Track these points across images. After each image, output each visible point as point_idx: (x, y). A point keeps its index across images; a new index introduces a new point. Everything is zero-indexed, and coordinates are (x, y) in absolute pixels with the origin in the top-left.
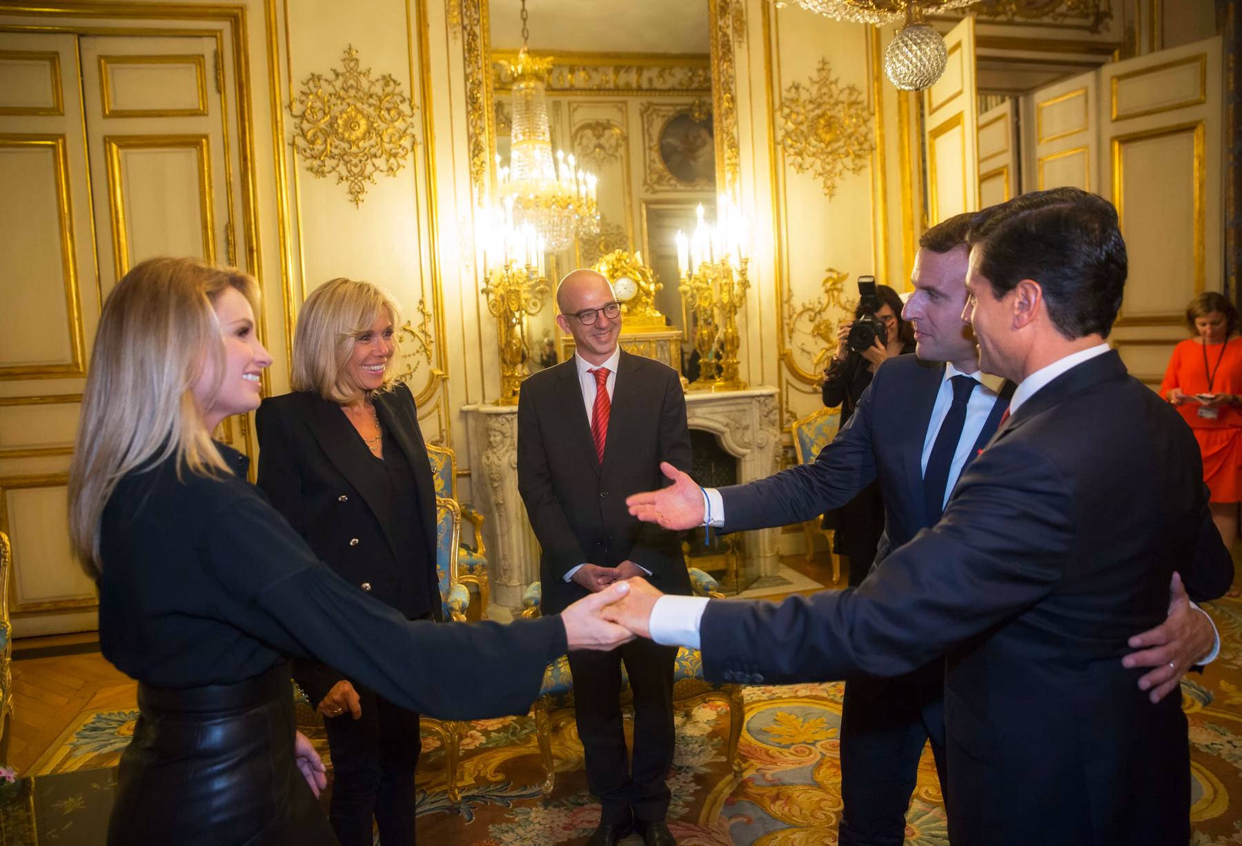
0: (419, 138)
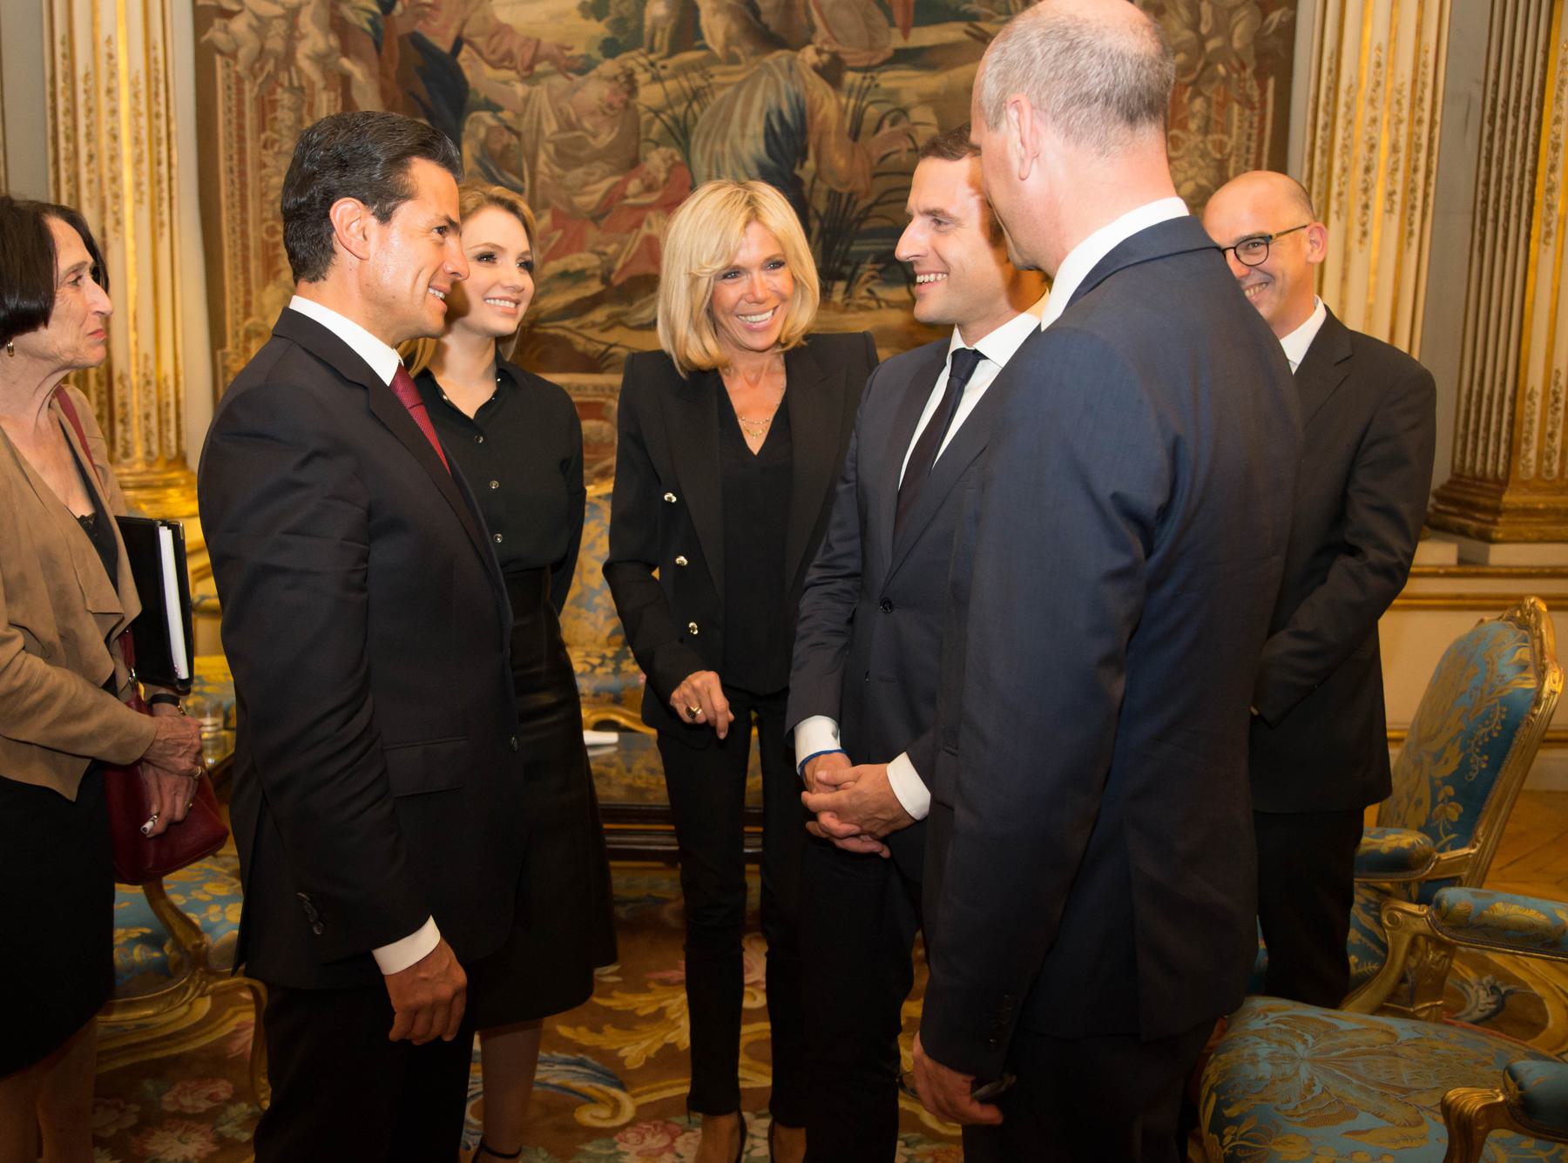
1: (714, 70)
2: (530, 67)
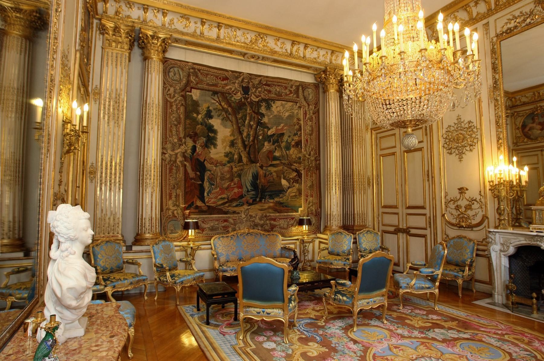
0: (480, 139)
1: (244, 166)
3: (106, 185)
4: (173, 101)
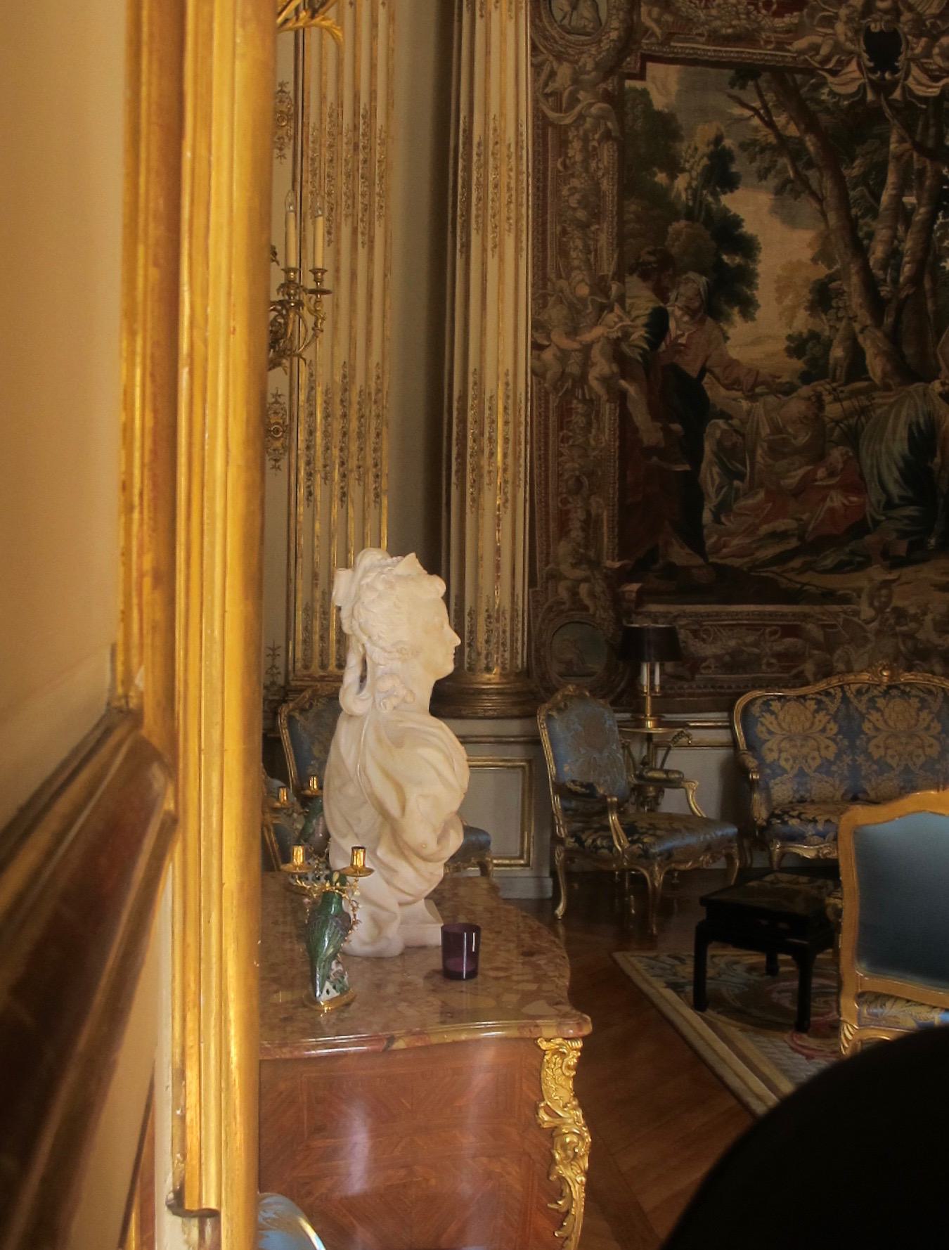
1: (875, 394)
2: (752, 389)
3: (327, 478)
4: (568, 121)
